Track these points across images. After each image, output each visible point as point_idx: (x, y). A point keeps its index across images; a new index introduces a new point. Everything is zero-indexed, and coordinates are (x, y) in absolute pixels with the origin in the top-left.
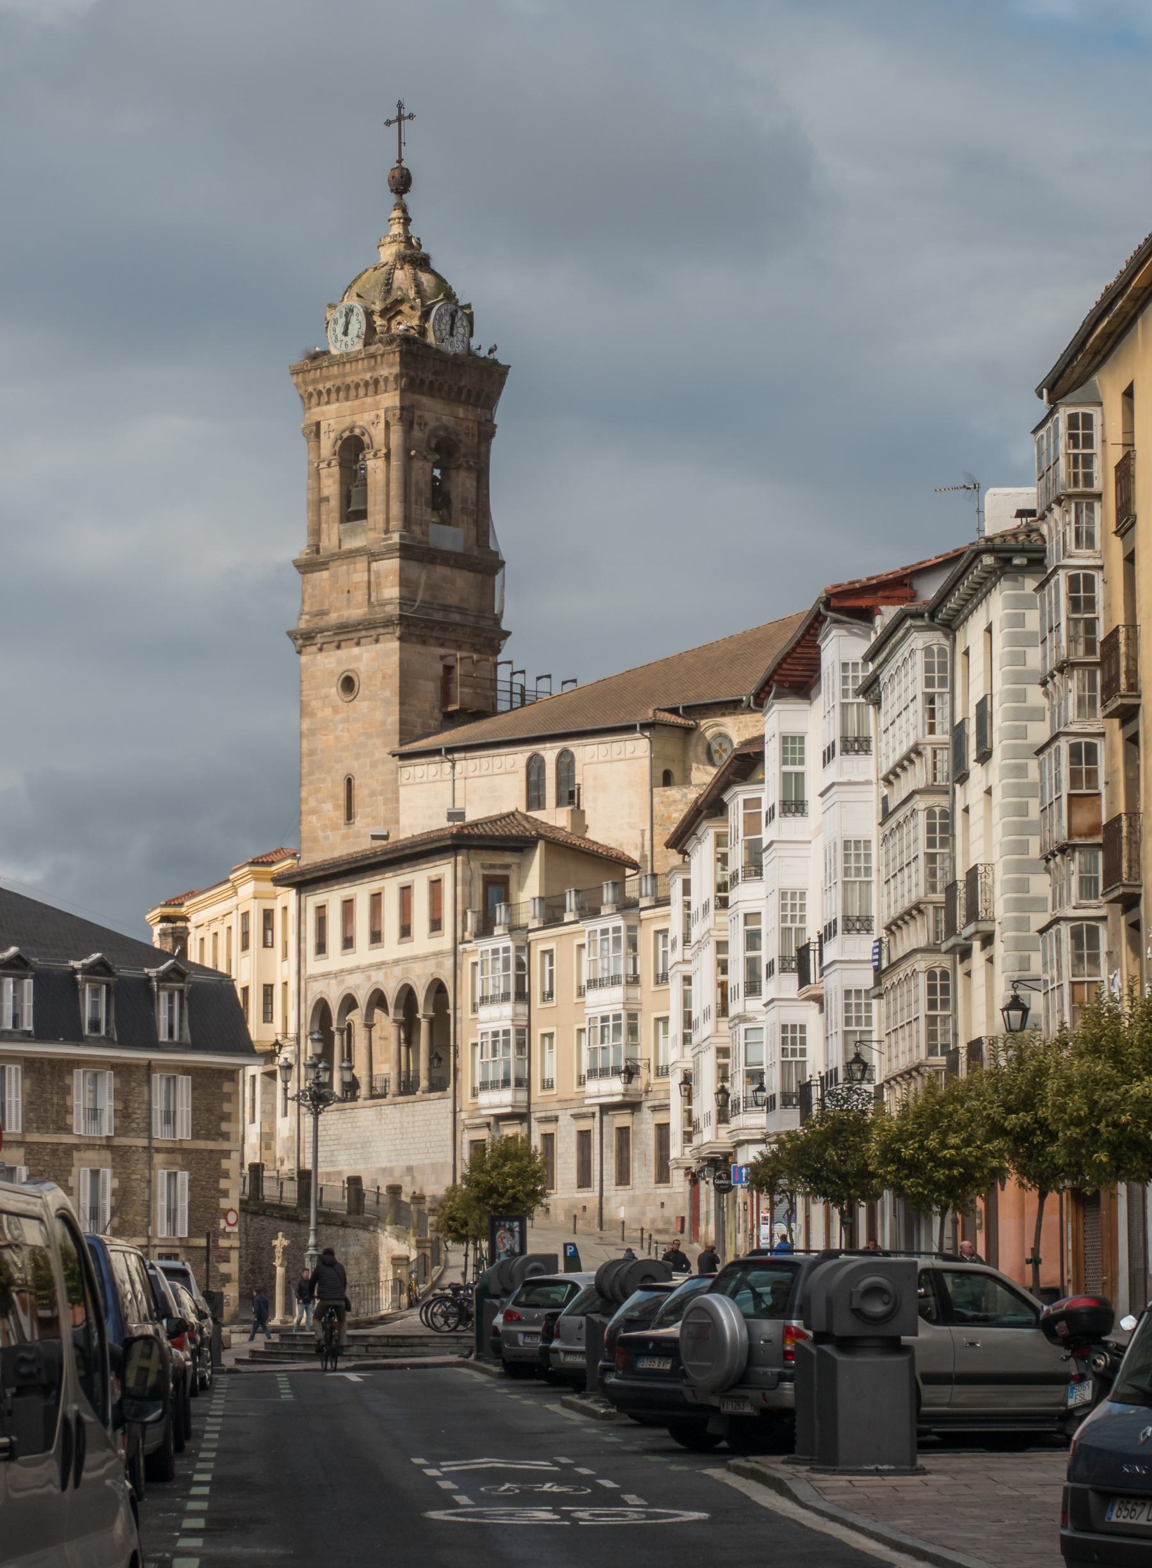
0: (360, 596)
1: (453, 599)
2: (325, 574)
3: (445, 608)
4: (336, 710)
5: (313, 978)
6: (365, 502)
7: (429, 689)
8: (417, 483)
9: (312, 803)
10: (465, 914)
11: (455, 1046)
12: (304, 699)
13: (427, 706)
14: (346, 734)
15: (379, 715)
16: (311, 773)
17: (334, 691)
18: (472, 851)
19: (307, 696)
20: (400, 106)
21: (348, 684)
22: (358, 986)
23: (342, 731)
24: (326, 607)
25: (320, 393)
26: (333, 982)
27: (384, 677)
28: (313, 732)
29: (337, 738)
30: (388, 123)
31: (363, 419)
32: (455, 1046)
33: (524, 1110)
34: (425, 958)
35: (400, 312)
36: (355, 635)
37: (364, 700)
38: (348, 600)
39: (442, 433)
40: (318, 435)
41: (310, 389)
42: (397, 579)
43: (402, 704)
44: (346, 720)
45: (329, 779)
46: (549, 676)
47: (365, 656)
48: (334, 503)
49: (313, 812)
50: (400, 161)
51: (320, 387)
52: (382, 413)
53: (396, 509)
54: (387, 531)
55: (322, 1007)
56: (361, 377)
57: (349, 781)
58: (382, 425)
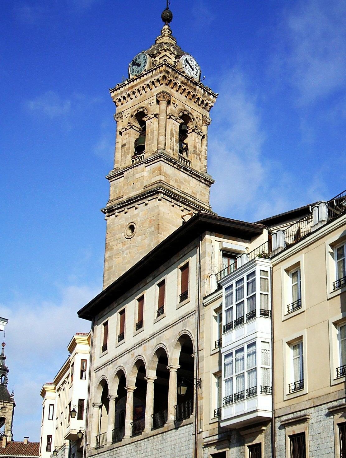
0: (138, 185)
1: (189, 192)
3: (184, 193)
4: (124, 244)
5: (98, 369)
19: (109, 240)
22: (125, 363)
23: (126, 254)
24: (122, 194)
25: (124, 98)
26: (111, 366)
28: (111, 258)
29: (124, 258)
33: (269, 415)
36: (136, 205)
37: (139, 235)
39: (185, 113)
44: (129, 248)
50: (167, 9)
56: (144, 83)
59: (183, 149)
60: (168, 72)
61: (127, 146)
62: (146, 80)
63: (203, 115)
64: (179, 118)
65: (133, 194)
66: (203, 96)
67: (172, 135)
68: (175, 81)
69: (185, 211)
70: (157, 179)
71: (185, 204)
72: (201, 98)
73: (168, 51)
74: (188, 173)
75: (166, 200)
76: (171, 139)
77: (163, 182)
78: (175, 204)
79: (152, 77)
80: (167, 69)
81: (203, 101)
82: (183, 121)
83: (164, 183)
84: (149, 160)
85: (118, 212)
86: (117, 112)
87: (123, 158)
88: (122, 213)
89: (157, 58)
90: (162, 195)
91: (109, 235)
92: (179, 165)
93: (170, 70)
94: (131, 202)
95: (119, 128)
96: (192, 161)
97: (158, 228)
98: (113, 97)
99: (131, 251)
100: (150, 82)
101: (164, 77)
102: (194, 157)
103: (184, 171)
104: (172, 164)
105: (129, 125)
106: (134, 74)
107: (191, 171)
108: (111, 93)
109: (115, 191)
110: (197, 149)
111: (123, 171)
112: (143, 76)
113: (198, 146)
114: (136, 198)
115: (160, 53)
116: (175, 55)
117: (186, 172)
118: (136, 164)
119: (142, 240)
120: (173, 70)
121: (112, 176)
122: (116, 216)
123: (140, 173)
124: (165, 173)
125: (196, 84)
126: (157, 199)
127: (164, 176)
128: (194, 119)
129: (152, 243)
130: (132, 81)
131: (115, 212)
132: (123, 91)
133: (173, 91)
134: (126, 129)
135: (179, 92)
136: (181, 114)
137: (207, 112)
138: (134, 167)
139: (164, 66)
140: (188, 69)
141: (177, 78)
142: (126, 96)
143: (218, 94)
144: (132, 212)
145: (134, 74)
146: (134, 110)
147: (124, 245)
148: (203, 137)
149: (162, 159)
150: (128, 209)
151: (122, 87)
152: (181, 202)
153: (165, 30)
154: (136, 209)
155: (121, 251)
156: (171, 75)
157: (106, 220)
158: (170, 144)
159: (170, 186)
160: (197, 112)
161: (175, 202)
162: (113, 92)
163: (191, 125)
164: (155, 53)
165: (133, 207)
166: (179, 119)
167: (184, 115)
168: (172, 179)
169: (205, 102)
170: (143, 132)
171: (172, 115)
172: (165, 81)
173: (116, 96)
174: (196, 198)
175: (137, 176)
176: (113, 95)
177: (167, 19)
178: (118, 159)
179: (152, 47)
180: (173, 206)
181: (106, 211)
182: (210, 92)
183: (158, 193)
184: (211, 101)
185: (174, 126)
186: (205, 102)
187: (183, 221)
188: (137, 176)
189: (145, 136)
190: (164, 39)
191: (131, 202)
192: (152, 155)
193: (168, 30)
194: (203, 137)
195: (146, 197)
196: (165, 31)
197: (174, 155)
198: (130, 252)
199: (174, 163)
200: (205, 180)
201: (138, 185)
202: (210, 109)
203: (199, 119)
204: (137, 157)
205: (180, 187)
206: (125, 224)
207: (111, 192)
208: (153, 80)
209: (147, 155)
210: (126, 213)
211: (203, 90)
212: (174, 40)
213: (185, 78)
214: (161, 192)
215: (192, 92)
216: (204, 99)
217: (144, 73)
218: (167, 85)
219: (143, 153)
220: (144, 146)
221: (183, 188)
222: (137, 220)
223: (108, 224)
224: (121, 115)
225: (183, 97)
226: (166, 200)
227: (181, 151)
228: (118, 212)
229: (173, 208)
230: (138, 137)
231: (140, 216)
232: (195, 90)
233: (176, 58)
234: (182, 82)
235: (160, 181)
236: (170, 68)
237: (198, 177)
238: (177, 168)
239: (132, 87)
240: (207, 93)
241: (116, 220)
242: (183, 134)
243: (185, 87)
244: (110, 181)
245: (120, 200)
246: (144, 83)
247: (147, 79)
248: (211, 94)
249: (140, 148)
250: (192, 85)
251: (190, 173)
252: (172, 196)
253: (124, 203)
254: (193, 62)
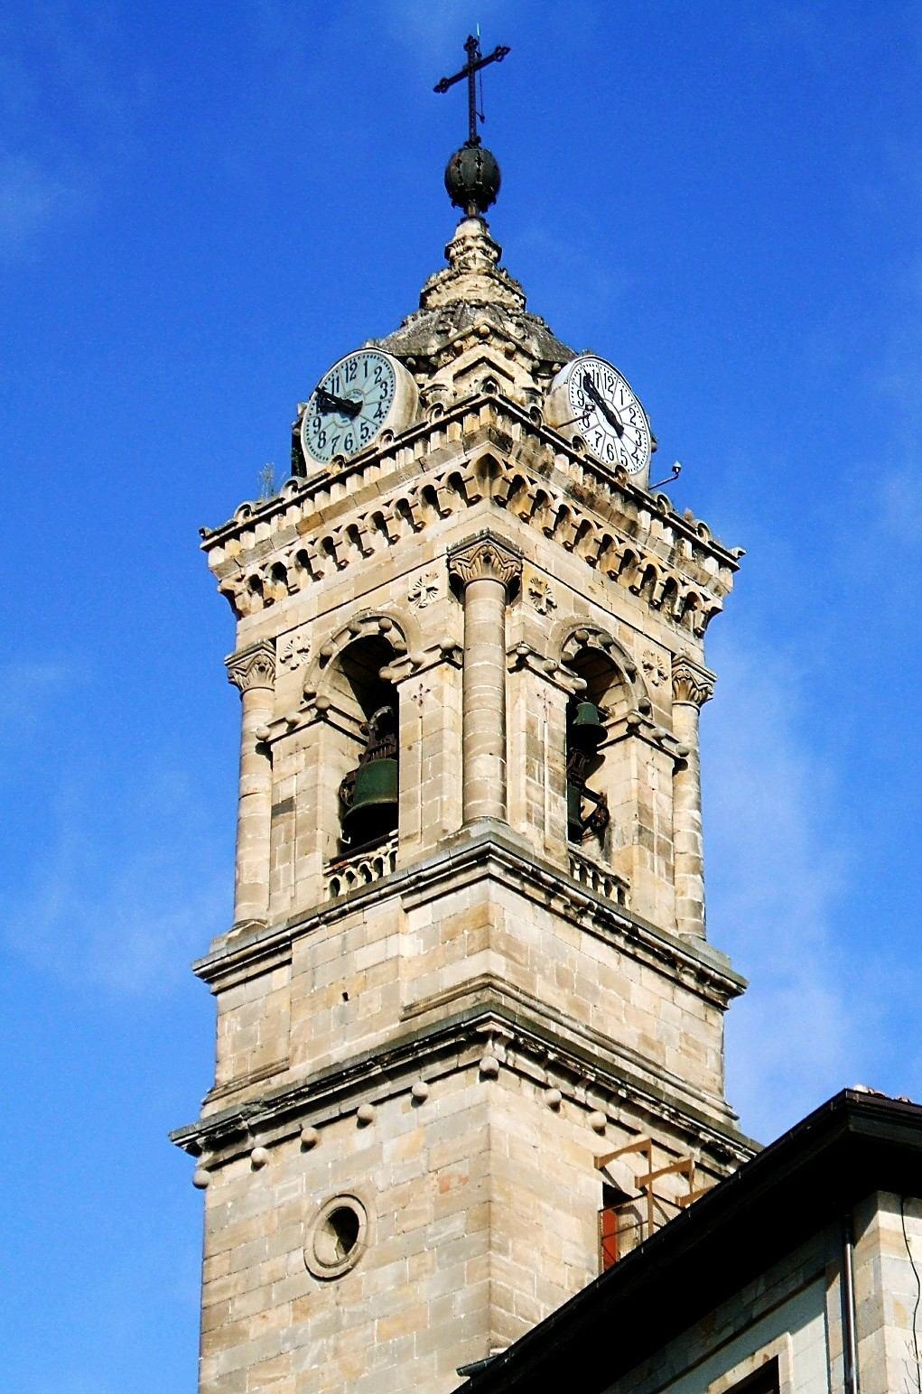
0: (371, 1001)
4: (302, 1307)
14: (333, 1364)
19: (223, 1289)
20: (471, 44)
23: (320, 1359)
25: (279, 572)
27: (445, 1189)
30: (443, 86)
31: (386, 601)
36: (363, 1103)
37: (382, 1262)
38: (343, 1018)
39: (594, 642)
44: (334, 1327)
47: (389, 1147)
50: (474, 142)
56: (385, 499)
59: (589, 823)
60: (504, 442)
61: (302, 809)
62: (394, 480)
63: (673, 655)
64: (562, 667)
65: (344, 1049)
66: (671, 559)
67: (535, 750)
68: (541, 485)
69: (612, 1130)
70: (472, 968)
71: (609, 1096)
72: (664, 570)
73: (494, 341)
74: (620, 941)
75: (522, 1075)
76: (529, 767)
77: (500, 984)
78: (564, 1096)
79: (422, 464)
80: (499, 426)
81: (671, 586)
82: (583, 683)
83: (508, 988)
84: (426, 873)
85: (268, 1146)
86: (241, 645)
87: (281, 867)
88: (285, 1147)
89: (444, 376)
90: (500, 1049)
91: (218, 1265)
92: (575, 902)
93: (515, 431)
94: (335, 1090)
95: (258, 722)
96: (635, 883)
97: (485, 1218)
98: (221, 571)
99: (342, 1343)
100: (413, 491)
101: (488, 467)
102: (643, 860)
103: (599, 930)
104: (541, 896)
105: (307, 704)
106: (327, 452)
107: (633, 931)
108: (208, 549)
109: (243, 1039)
110: (656, 822)
111: (288, 933)
112: (376, 462)
113: (660, 803)
114: (362, 1068)
115: (459, 352)
116: (531, 357)
117: (608, 936)
118: (353, 895)
119: (401, 1281)
120: (529, 430)
121: (227, 960)
122: (257, 1166)
123: (379, 946)
124: (509, 939)
125: (636, 499)
126: (475, 1072)
127: (506, 954)
128: (632, 674)
130: (318, 490)
131: (247, 1147)
132: (274, 539)
133: (530, 537)
134: (293, 728)
135: (560, 537)
136: (573, 648)
137: (692, 638)
138: (344, 913)
139: (485, 410)
140: (599, 429)
141: (545, 469)
142: (286, 562)
143: (740, 553)
144: (342, 1141)
145: (327, 452)
146: (330, 632)
147: (306, 1312)
148: (680, 764)
149: (493, 869)
150: (319, 1126)
151: (267, 519)
152: (590, 1086)
153: (469, 243)
154: (363, 1123)
155: (288, 1346)
156: (518, 458)
157: (203, 1187)
158: (528, 795)
159: (539, 1007)
160: (644, 637)
161: (565, 1086)
162: (221, 543)
163: (619, 704)
164: (431, 351)
165: (343, 1116)
166: (563, 672)
167: (586, 652)
168: (542, 970)
169: (683, 592)
170: (382, 735)
171: (532, 653)
172: (491, 483)
173: (237, 562)
174: (659, 1067)
175: (364, 957)
176: (217, 557)
177: (474, 193)
178: (256, 875)
179: (412, 325)
180: (555, 1107)
181: (200, 1141)
182: (704, 540)
183: (482, 1039)
184: (711, 586)
185: (540, 704)
186: (683, 592)
187: (605, 1186)
188: (364, 957)
189: (396, 756)
190: (465, 287)
191: (335, 1090)
192: (438, 851)
193: (481, 243)
194: (680, 764)
195: (418, 1064)
196: (469, 248)
197: (546, 849)
198: (337, 1352)
199: (554, 891)
200: (702, 977)
201: (371, 1001)
202: (705, 624)
203: (655, 672)
204: (355, 864)
205: (582, 1009)
206: (306, 1205)
207: (225, 1045)
208: (427, 479)
209: (412, 848)
210: (308, 1146)
211: (669, 530)
212: (514, 292)
213: (587, 470)
214: (497, 1036)
215: (621, 541)
216: (677, 574)
217: (384, 447)
218: (500, 502)
219: (389, 845)
220: (393, 809)
221: (600, 1019)
222: (369, 1183)
223: (211, 1205)
224: (262, 657)
225: (575, 566)
226: (522, 1075)
227: (575, 834)
228: (268, 1146)
229: (555, 1115)
230: (353, 765)
231: (385, 1160)
232: (633, 528)
233: (534, 373)
234: (573, 492)
235: (488, 982)
236: (515, 419)
237: (666, 959)
238: (564, 917)
239: (322, 517)
240: (688, 545)
241: (255, 1186)
242: (584, 744)
243: (587, 515)
244: (215, 987)
245: (276, 1081)
247: (400, 476)
248: (708, 553)
249: (368, 820)
250: (618, 505)
251: (628, 940)
252: (551, 1056)
253: (296, 1098)
254: (618, 394)
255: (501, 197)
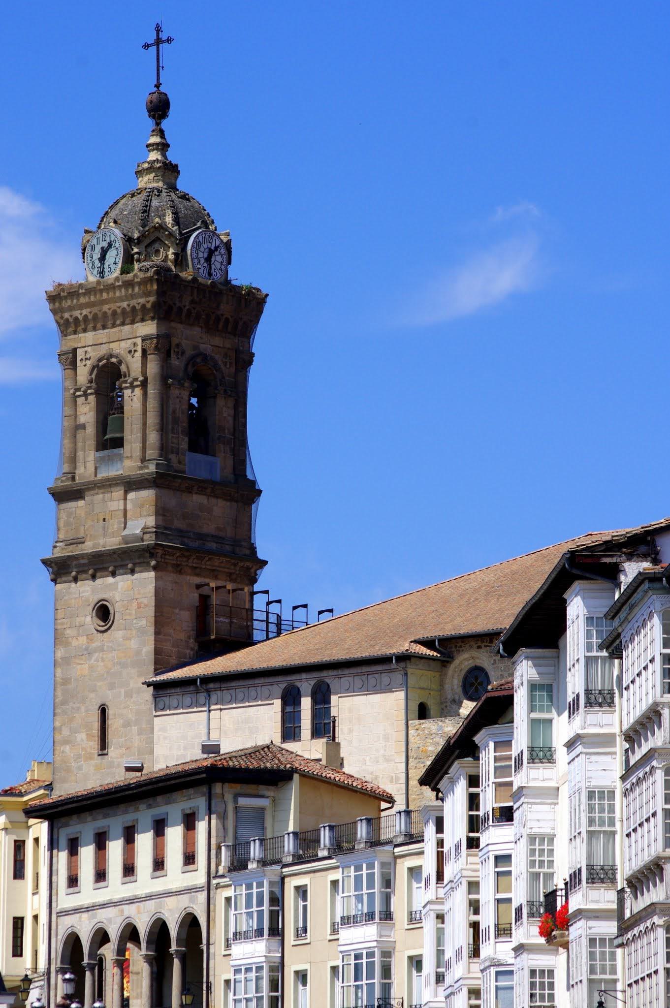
1: (209, 528)
2: (81, 503)
3: (202, 537)
4: (90, 639)
6: (121, 429)
7: (185, 620)
8: (174, 412)
9: (66, 732)
10: (219, 848)
11: (208, 982)
12: (59, 627)
13: (182, 636)
15: (133, 644)
16: (64, 703)
17: (90, 620)
18: (227, 785)
19: (62, 624)
20: (158, 30)
21: (103, 612)
22: (110, 920)
24: (82, 535)
31: (120, 348)
32: (208, 982)
34: (178, 893)
35: (158, 239)
38: (104, 528)
40: (73, 365)
41: (66, 315)
42: (153, 509)
43: (157, 633)
45: (83, 709)
46: (305, 606)
47: (120, 585)
48: (91, 430)
49: (66, 742)
50: (158, 86)
51: (77, 313)
52: (139, 341)
53: (153, 437)
54: (143, 460)
55: (73, 942)
57: (103, 711)
58: (139, 354)
101: (156, 306)
129: (144, 650)
198: (102, 658)
246: (118, 304)
255: (172, 112)
